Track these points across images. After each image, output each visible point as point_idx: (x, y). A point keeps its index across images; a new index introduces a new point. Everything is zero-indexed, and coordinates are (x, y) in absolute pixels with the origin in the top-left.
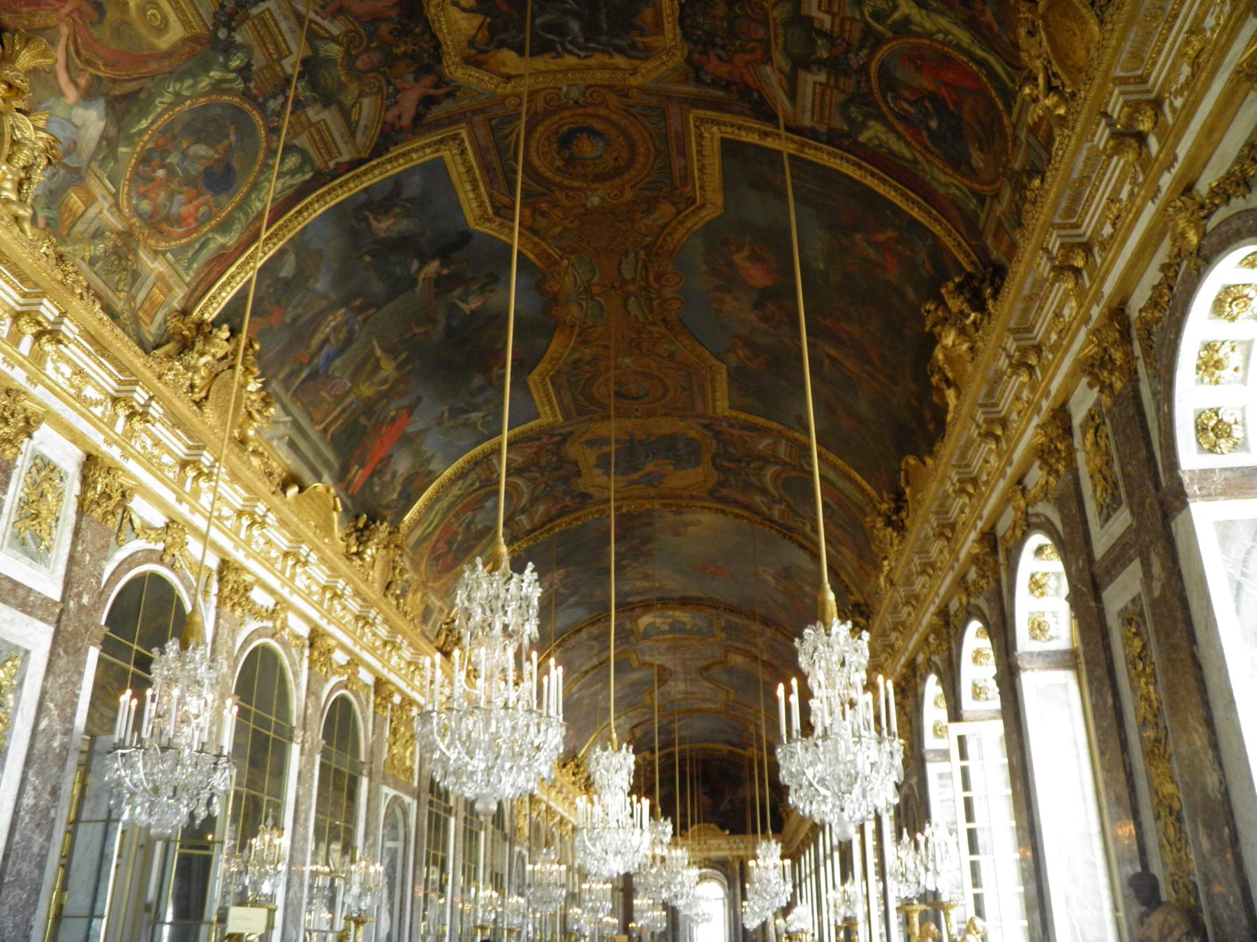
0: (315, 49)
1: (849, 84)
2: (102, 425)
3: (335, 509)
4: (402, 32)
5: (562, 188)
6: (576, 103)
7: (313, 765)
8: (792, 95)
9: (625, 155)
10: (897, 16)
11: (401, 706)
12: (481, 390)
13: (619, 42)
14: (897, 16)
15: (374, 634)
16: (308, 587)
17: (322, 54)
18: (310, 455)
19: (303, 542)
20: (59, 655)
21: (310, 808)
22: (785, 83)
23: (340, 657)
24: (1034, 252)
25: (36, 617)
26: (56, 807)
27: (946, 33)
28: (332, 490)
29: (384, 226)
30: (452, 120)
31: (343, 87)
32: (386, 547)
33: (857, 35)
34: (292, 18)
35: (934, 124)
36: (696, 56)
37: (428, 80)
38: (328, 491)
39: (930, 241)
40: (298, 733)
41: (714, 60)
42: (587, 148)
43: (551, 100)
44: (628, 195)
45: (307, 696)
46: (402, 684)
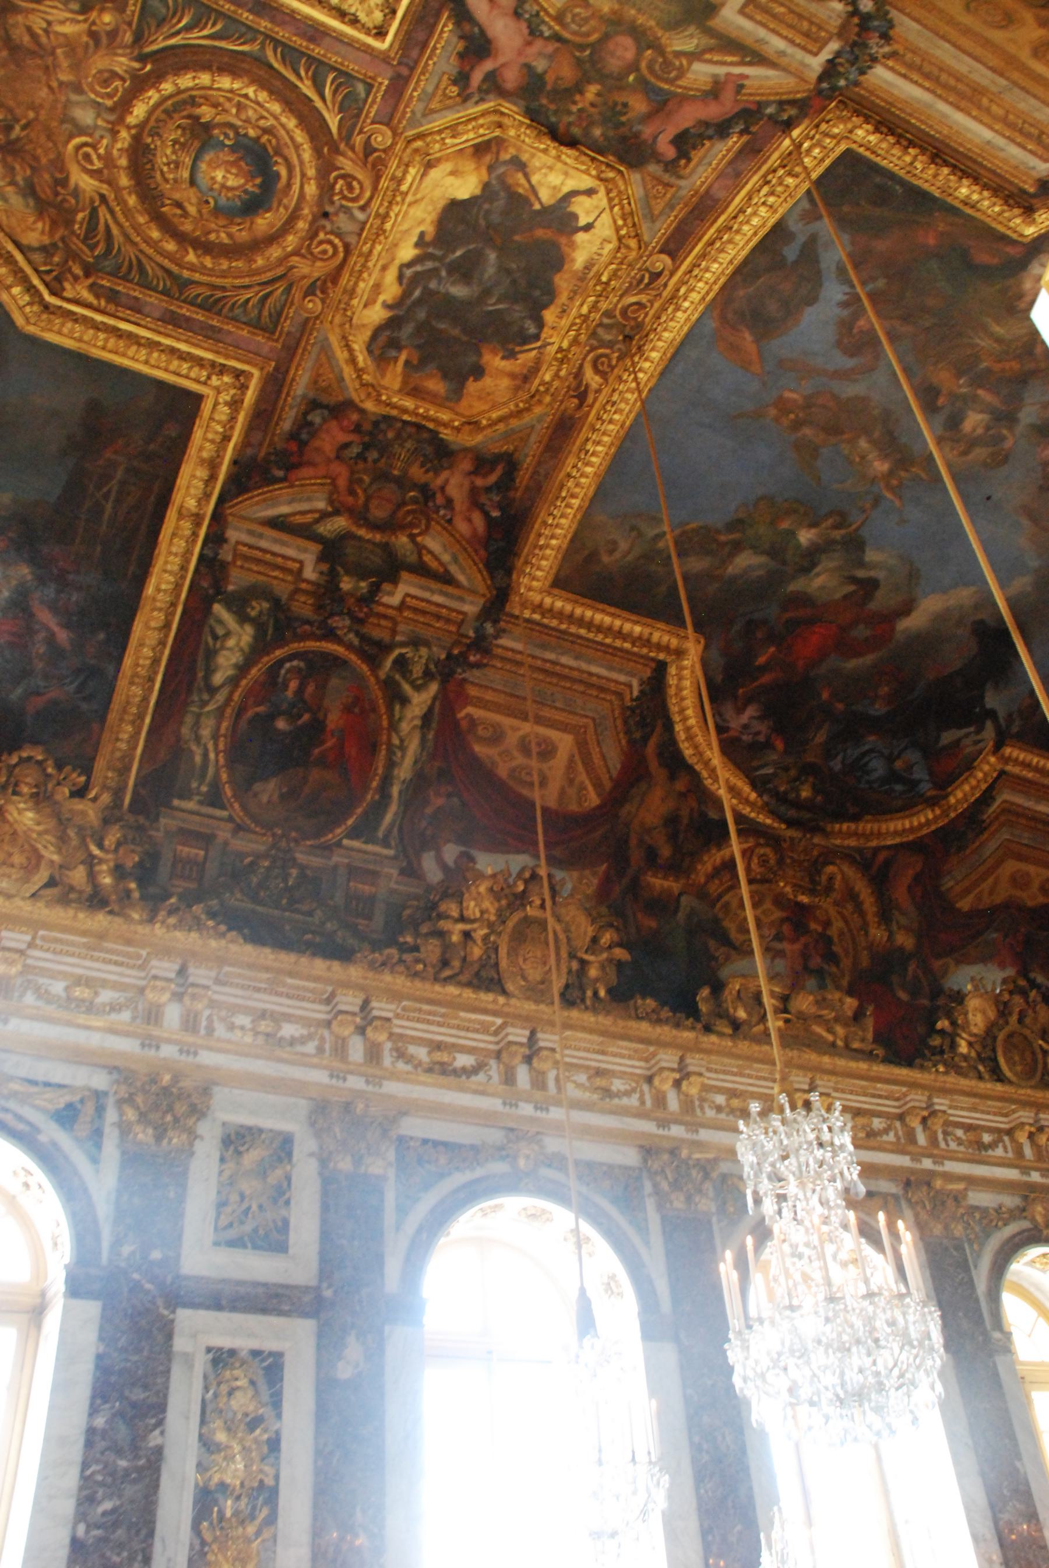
0: (711, 32)
1: (303, 607)
5: (139, 85)
6: (326, 215)
8: (277, 524)
9: (187, 227)
10: (406, 687)
13: (408, 329)
14: (406, 687)
17: (692, 29)
22: (299, 519)
24: (362, 988)
27: (403, 748)
33: (377, 634)
34: (773, 57)
35: (281, 724)
36: (355, 417)
37: (511, 78)
39: (85, 706)
41: (343, 438)
42: (224, 176)
43: (351, 189)
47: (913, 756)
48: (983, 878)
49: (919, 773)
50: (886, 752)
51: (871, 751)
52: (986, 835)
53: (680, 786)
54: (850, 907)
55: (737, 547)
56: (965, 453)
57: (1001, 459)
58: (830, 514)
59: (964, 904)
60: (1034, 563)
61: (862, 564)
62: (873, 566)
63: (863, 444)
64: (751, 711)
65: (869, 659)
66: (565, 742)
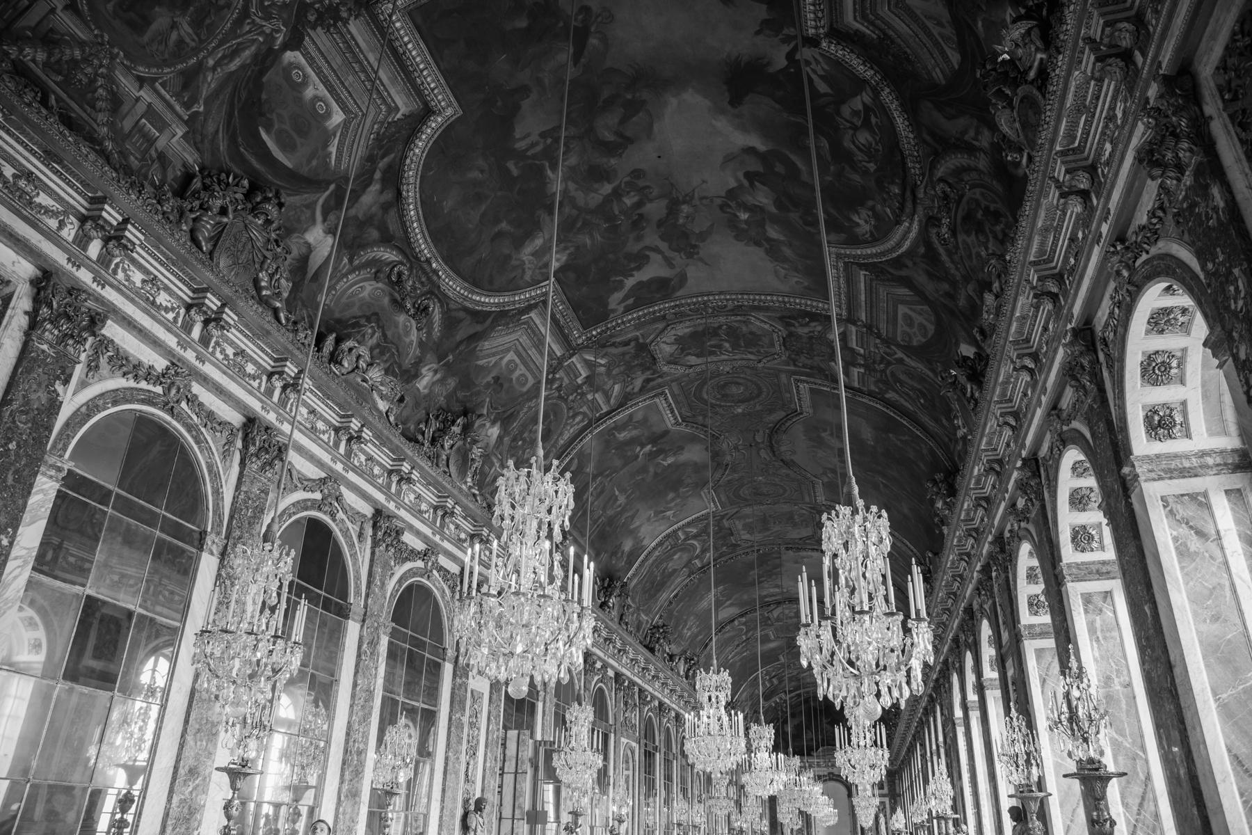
4: (636, 356)
5: (720, 406)
11: (628, 687)
12: (673, 500)
23: (598, 665)
29: (622, 436)
30: (660, 386)
31: (605, 383)
33: (878, 359)
44: (758, 408)
46: (628, 674)
47: (846, 111)
48: (929, 34)
49: (857, 103)
50: (851, 132)
51: (854, 143)
52: (891, 33)
53: (910, 264)
54: (966, 178)
55: (769, 240)
56: (648, 187)
57: (637, 174)
58: (724, 212)
59: (955, 58)
60: (673, 102)
61: (741, 186)
62: (737, 180)
63: (681, 221)
64: (856, 218)
65: (793, 157)
66: (902, 309)
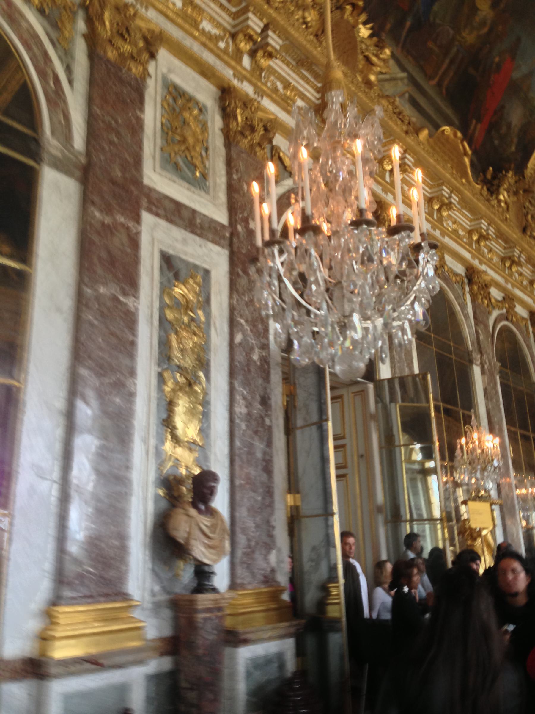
2: (226, 58)
3: (466, 154)
7: (495, 384)
15: (521, 274)
16: (455, 231)
18: (430, 111)
19: (442, 184)
20: (238, 275)
21: (502, 420)
23: (496, 294)
25: (208, 239)
26: (269, 416)
28: (459, 134)
32: (516, 193)
38: (455, 135)
40: (476, 356)
45: (476, 324)
